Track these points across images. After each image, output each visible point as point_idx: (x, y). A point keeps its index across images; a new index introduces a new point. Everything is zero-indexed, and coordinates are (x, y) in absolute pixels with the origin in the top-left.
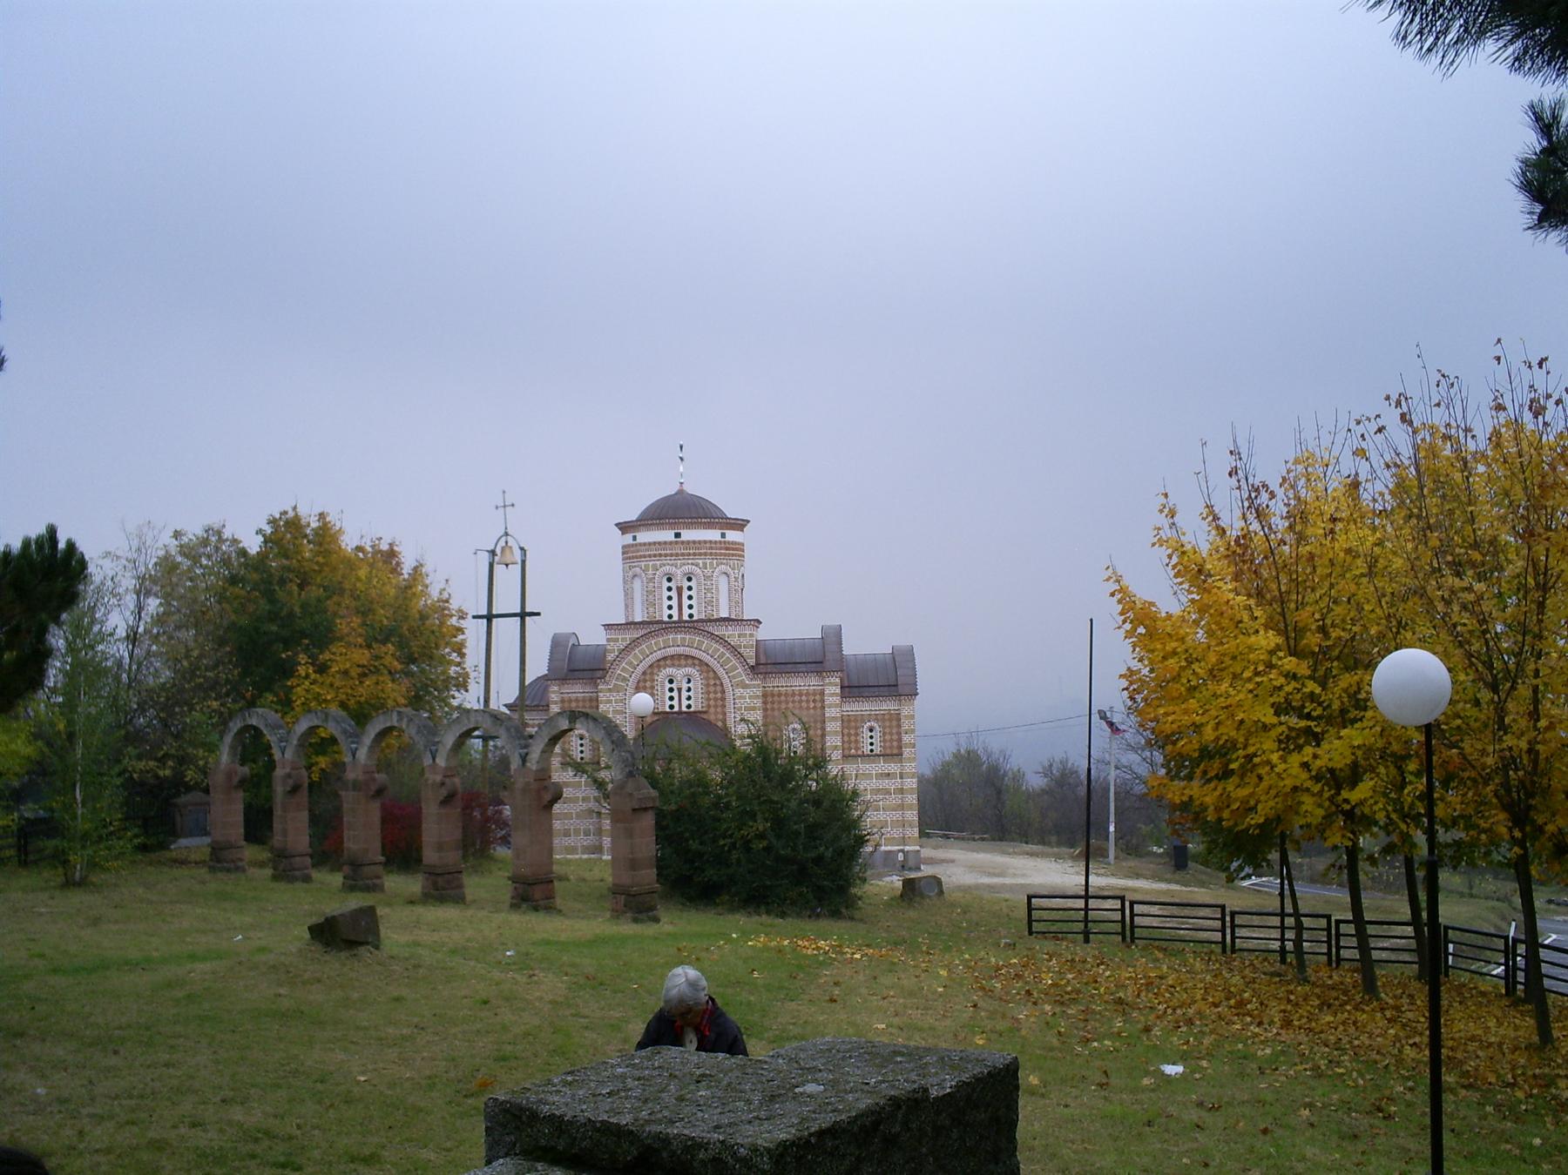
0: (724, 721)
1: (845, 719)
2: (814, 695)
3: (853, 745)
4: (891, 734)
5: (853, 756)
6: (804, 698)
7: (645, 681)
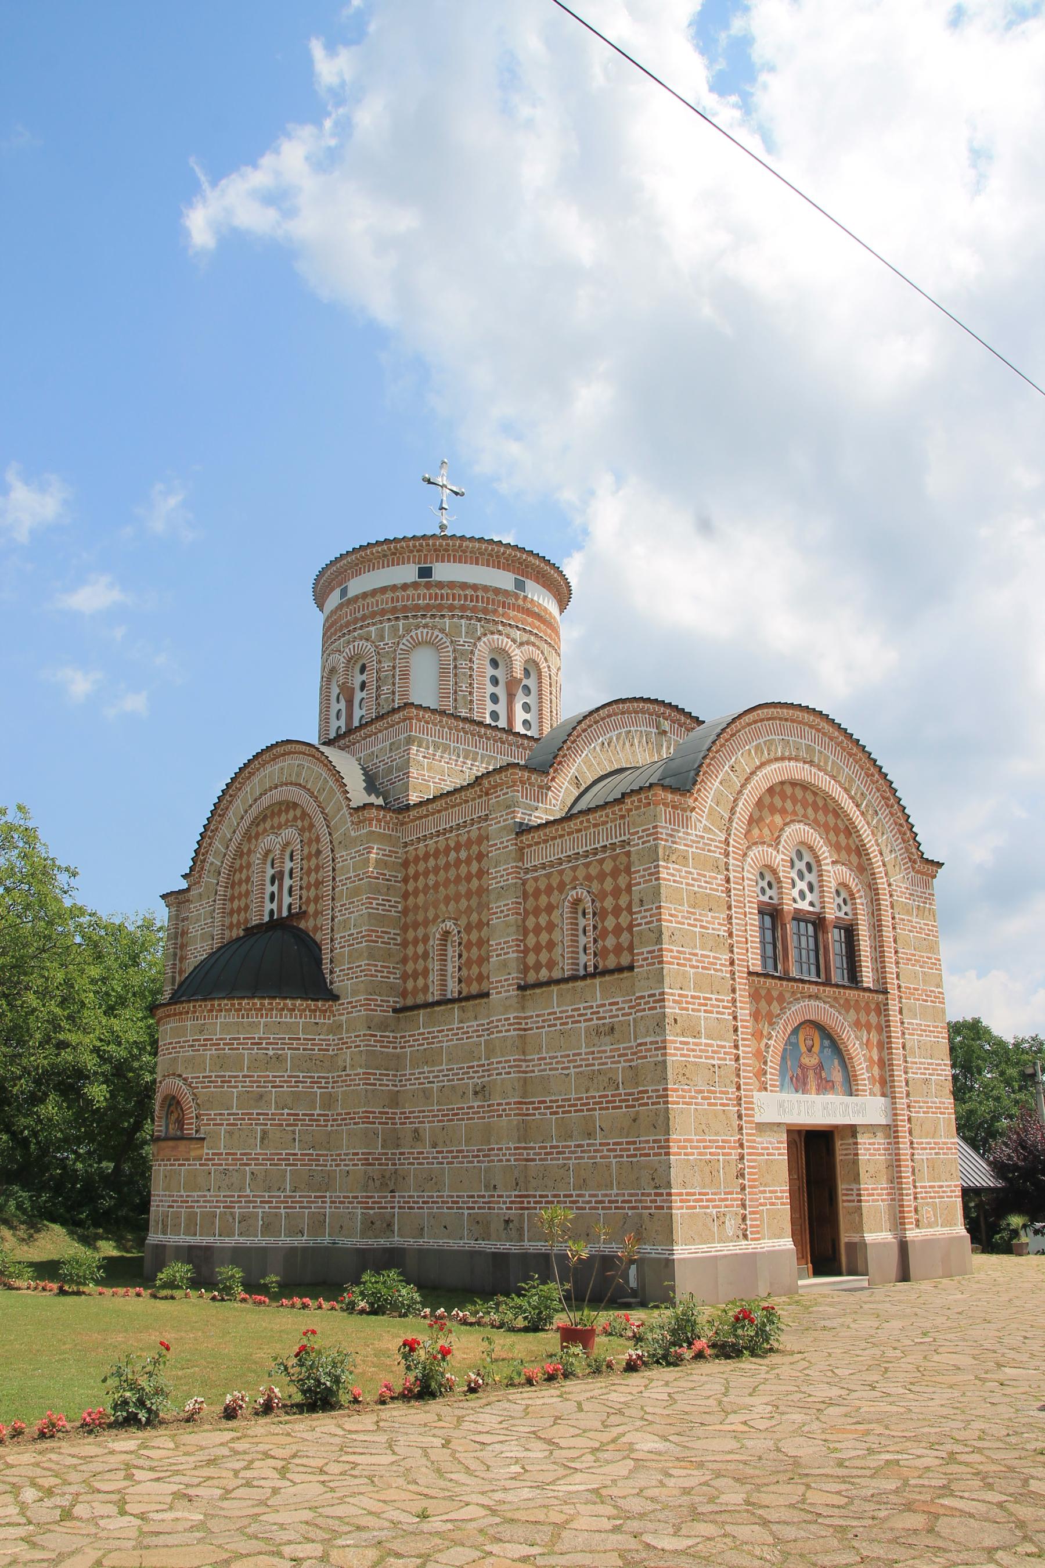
1: (530, 888)
5: (539, 985)
6: (463, 855)
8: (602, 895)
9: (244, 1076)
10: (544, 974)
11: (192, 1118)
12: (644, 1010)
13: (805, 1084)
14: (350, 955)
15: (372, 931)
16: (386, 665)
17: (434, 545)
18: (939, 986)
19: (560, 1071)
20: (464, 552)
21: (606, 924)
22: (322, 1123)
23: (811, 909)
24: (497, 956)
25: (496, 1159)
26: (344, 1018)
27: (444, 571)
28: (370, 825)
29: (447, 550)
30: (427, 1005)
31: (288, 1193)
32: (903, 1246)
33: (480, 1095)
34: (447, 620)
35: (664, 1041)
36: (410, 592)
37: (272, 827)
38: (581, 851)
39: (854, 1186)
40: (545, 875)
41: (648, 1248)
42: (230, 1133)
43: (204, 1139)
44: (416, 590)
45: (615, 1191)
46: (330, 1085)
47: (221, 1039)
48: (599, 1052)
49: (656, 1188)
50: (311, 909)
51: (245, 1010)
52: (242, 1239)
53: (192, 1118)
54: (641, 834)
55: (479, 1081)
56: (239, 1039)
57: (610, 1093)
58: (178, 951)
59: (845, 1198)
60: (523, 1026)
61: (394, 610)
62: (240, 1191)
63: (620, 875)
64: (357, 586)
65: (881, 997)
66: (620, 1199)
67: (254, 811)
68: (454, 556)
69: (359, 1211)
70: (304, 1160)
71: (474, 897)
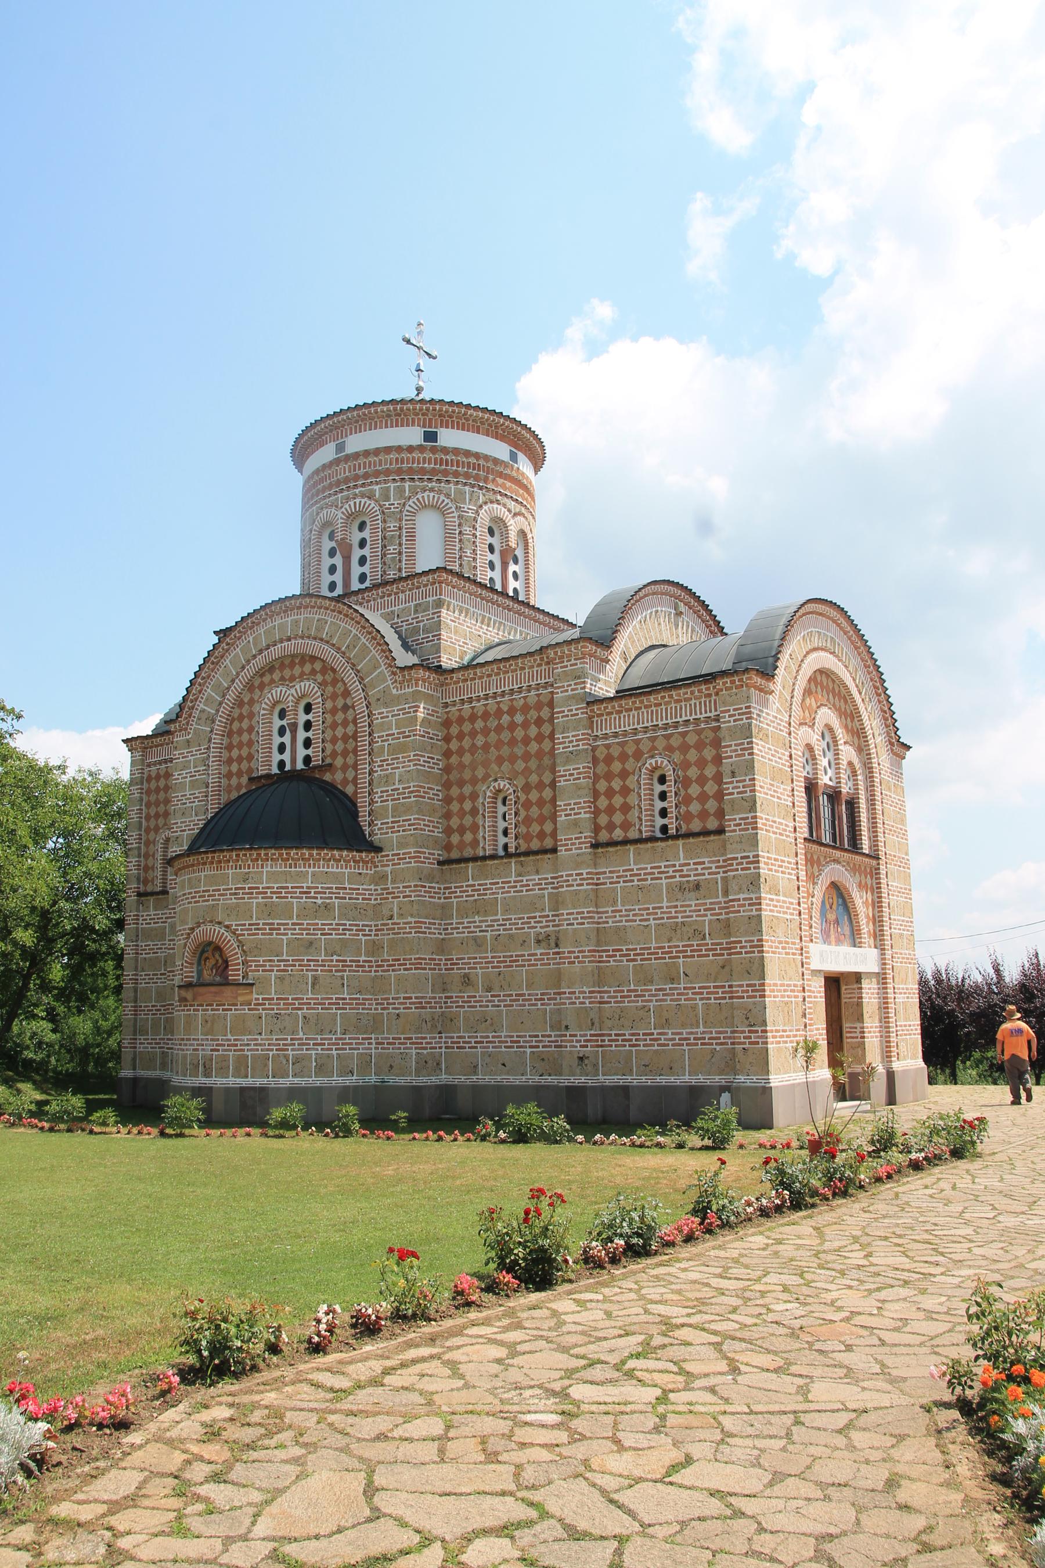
0: (355, 781)
1: (601, 754)
2: (539, 706)
3: (618, 818)
4: (702, 780)
6: (519, 718)
7: (241, 718)
8: (686, 765)
9: (293, 924)
10: (618, 834)
11: (238, 964)
12: (737, 870)
13: (828, 936)
14: (395, 809)
15: (421, 787)
16: (392, 525)
17: (441, 410)
18: (907, 854)
19: (638, 922)
20: (467, 420)
21: (690, 791)
22: (367, 969)
23: (830, 783)
24: (566, 815)
25: (567, 1001)
26: (389, 869)
27: (449, 437)
28: (417, 685)
29: (451, 417)
30: (475, 859)
31: (339, 1036)
32: (891, 1076)
33: (543, 944)
34: (451, 485)
35: (760, 898)
36: (416, 455)
37: (282, 679)
38: (660, 723)
39: (858, 1025)
40: (618, 743)
41: (741, 1078)
42: (281, 979)
43: (252, 985)
44: (421, 453)
45: (702, 1029)
46: (373, 933)
47: (268, 888)
48: (682, 906)
49: (751, 1026)
50: (339, 762)
51: (293, 859)
52: (296, 1080)
53: (238, 964)
54: (732, 712)
55: (542, 931)
56: (287, 888)
57: (695, 943)
58: (144, 796)
59: (849, 1035)
60: (595, 881)
61: (399, 471)
62: (293, 1034)
63: (705, 747)
64: (357, 442)
65: (874, 862)
66: (707, 1036)
67: (260, 661)
68: (458, 423)
69: (414, 1051)
70: (352, 1004)
71: (533, 759)
